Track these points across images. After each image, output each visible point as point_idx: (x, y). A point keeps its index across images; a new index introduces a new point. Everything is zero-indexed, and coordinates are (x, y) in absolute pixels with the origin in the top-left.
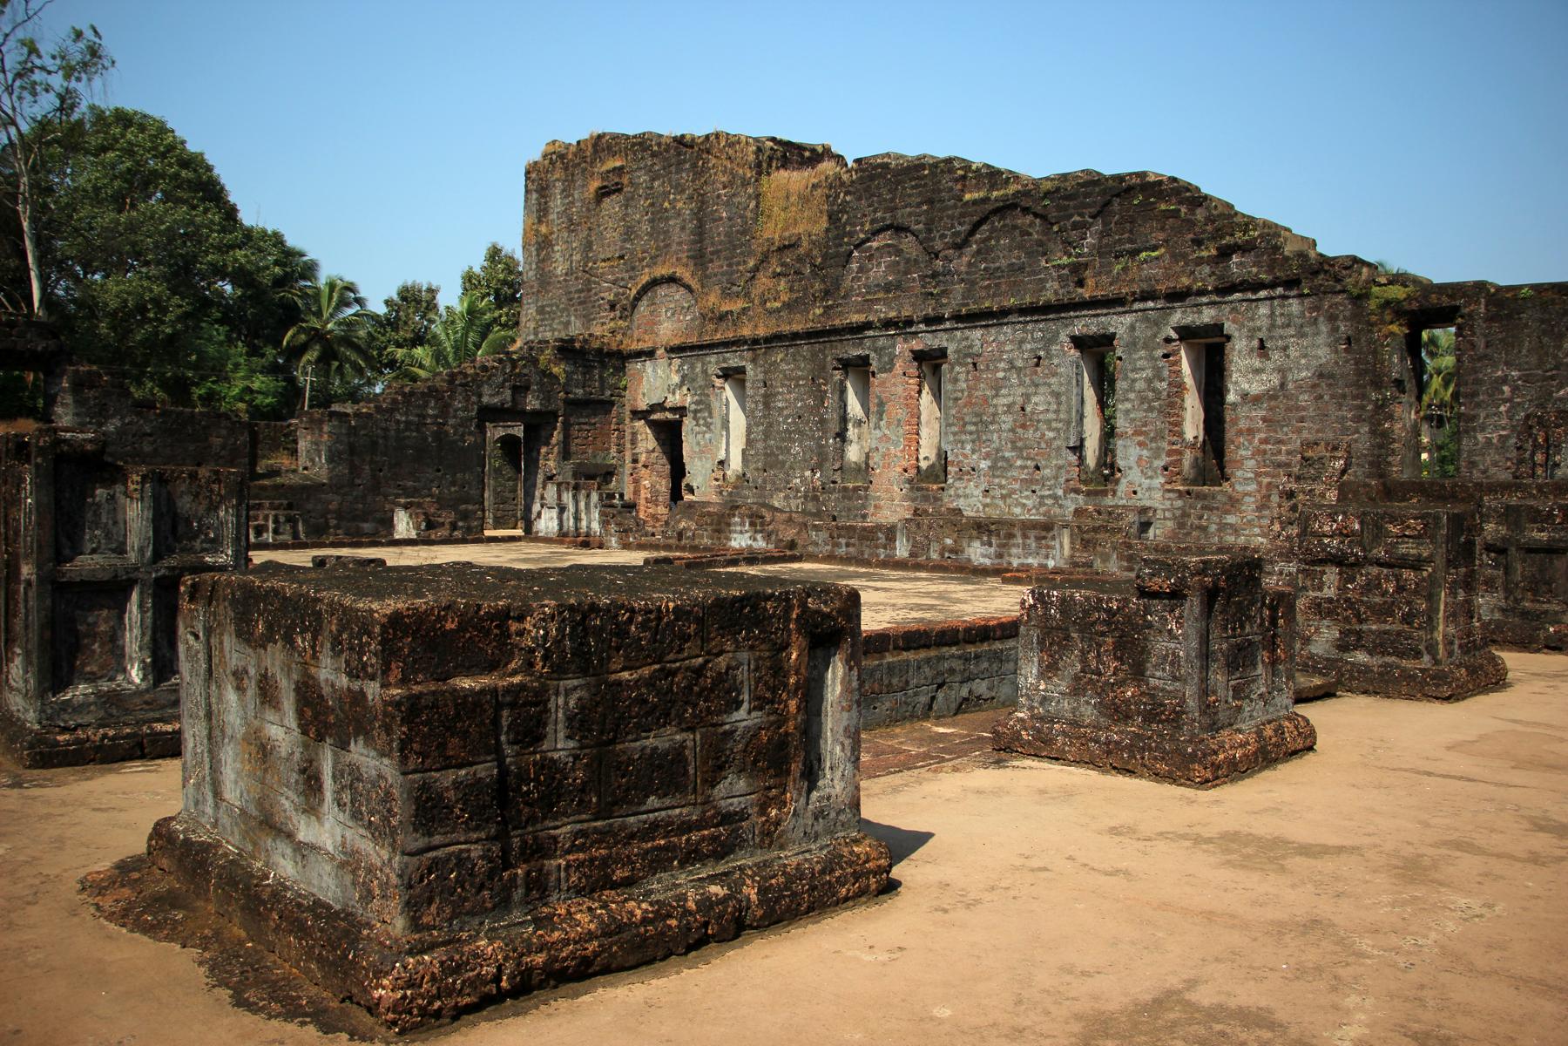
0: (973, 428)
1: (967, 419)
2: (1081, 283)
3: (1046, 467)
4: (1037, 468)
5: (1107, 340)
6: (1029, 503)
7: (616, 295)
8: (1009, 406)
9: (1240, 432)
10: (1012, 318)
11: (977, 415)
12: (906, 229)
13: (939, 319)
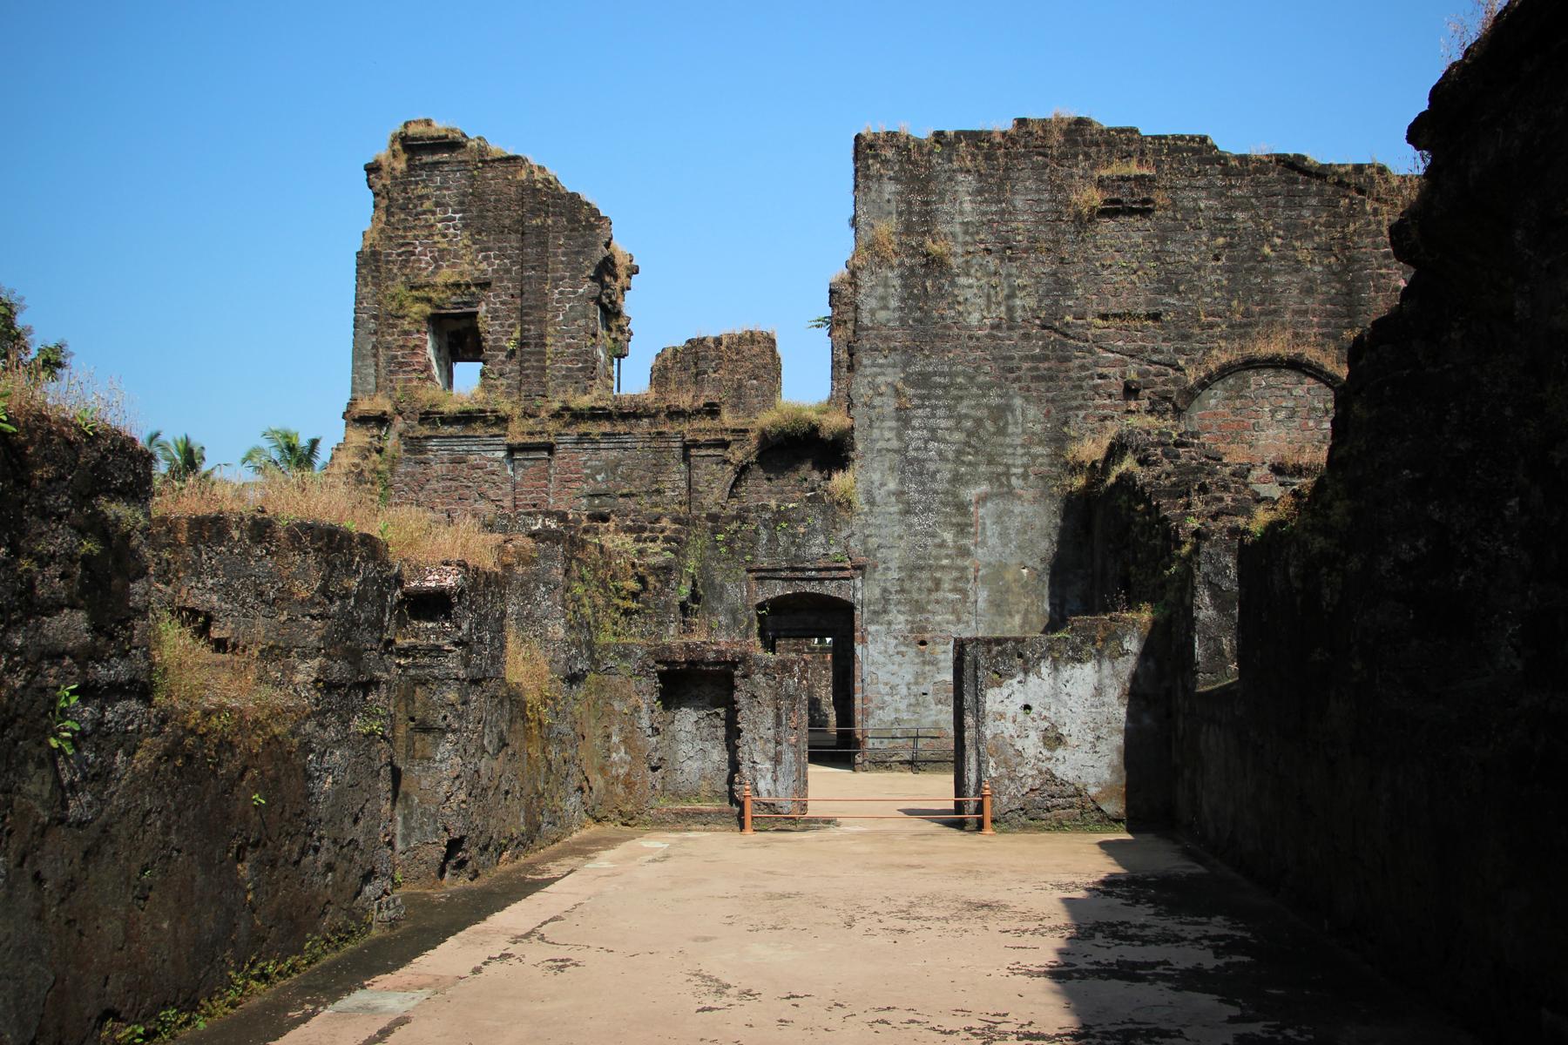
7: (1139, 374)
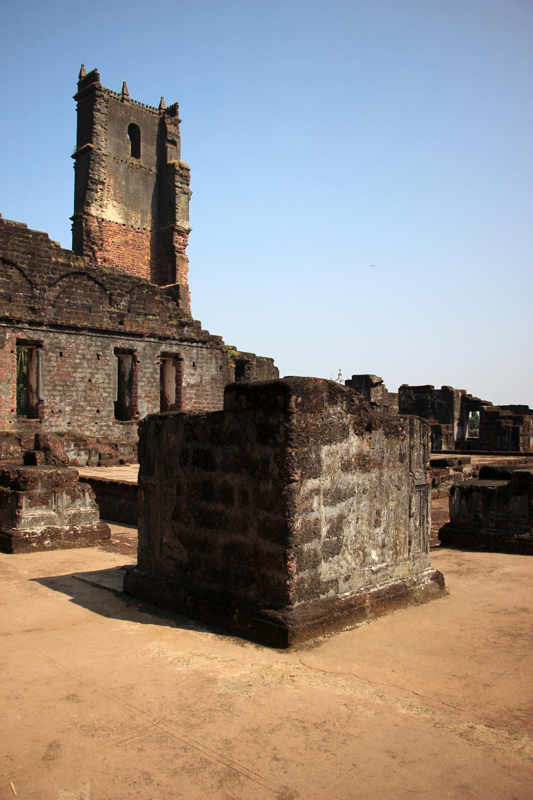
0: (61, 388)
1: (57, 383)
2: (121, 323)
3: (104, 411)
4: (98, 411)
5: (131, 352)
6: (94, 429)
8: (83, 378)
9: (187, 399)
10: (83, 332)
11: (63, 381)
12: (13, 264)
13: (41, 324)
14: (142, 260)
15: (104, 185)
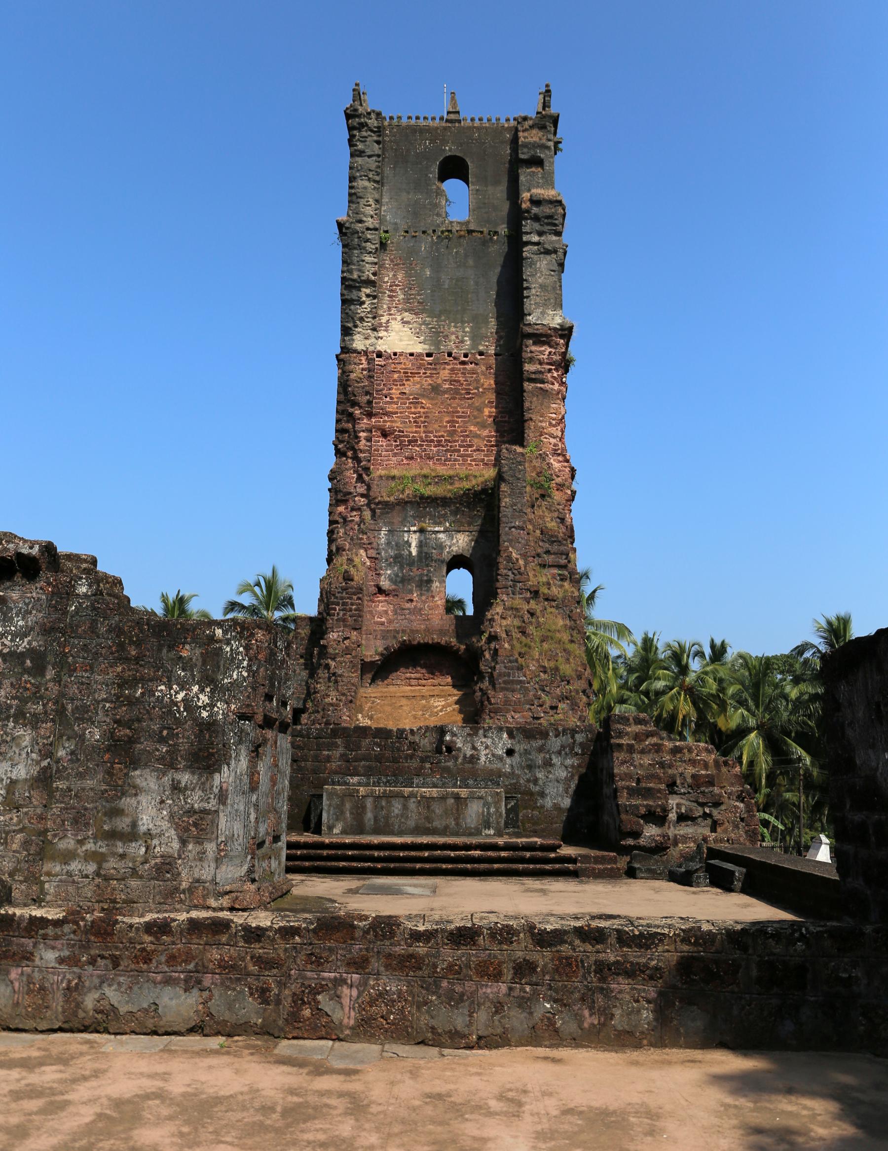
14: (475, 418)
15: (375, 287)
